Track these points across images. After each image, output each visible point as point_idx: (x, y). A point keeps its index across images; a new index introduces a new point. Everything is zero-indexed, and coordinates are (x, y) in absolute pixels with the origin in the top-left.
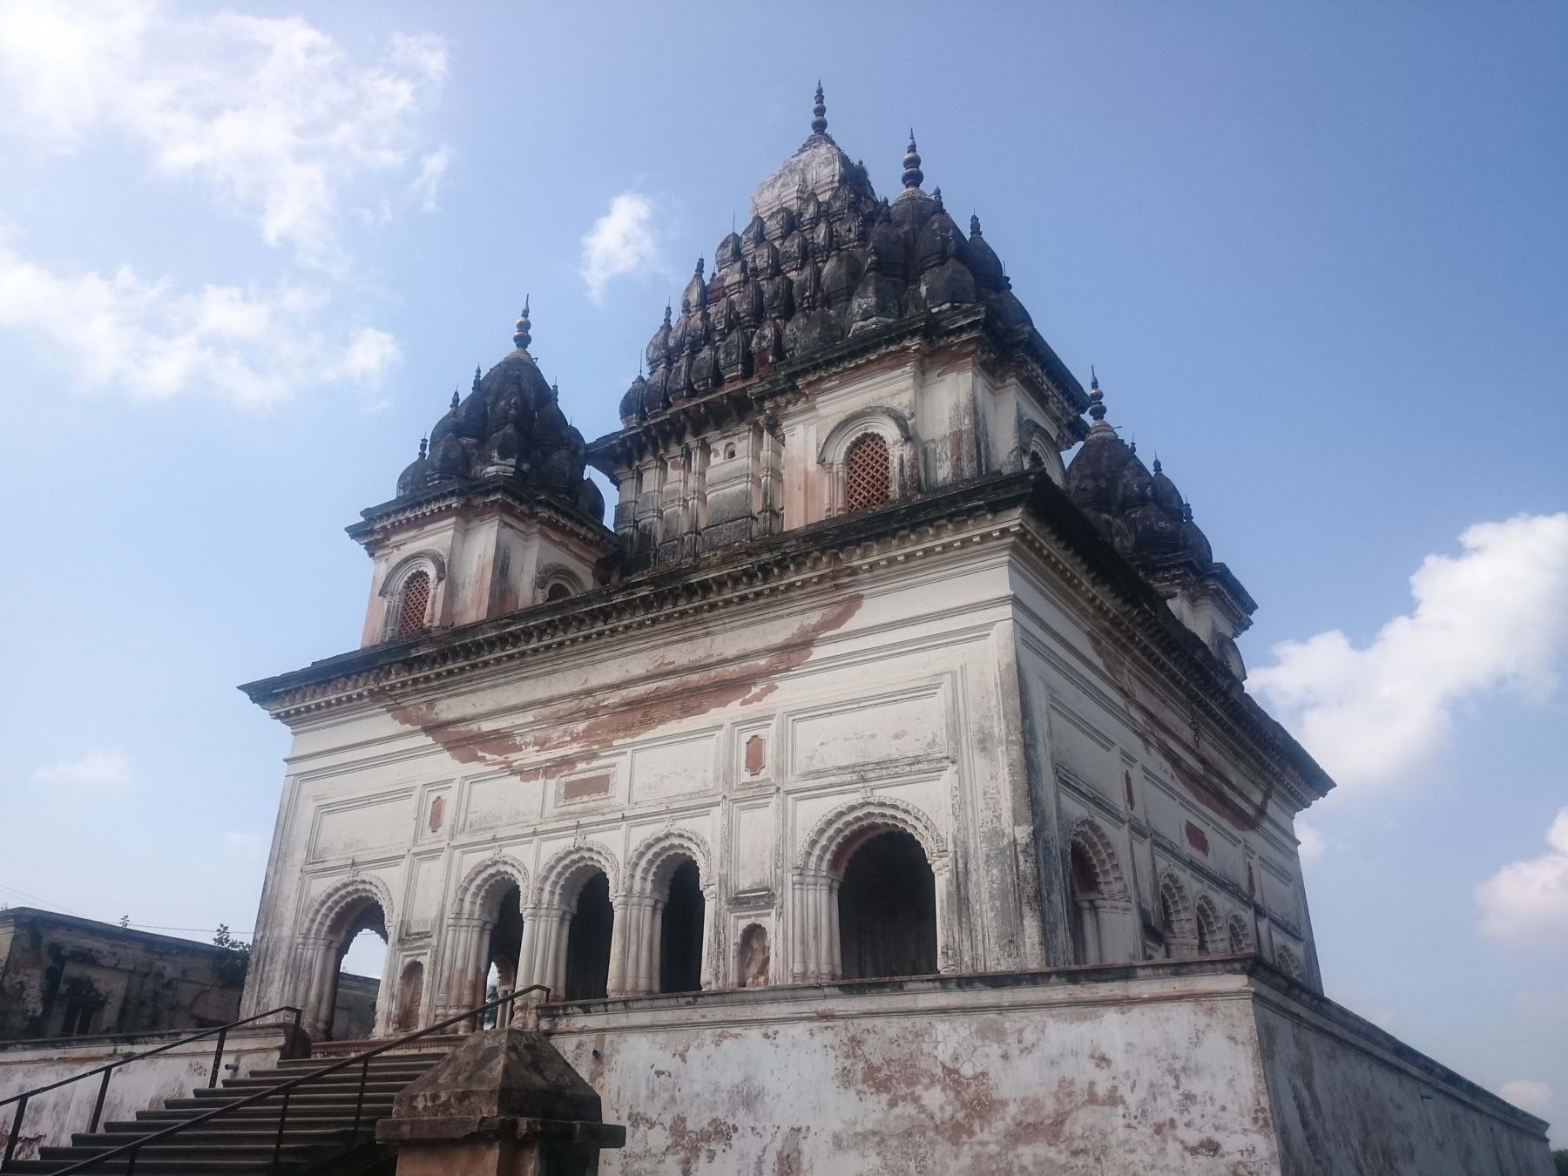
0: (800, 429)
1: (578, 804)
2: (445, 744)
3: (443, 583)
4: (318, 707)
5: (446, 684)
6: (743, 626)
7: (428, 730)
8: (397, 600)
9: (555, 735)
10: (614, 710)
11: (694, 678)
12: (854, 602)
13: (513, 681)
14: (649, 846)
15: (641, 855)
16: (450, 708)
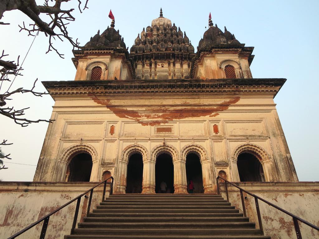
0: (209, 61)
1: (162, 134)
3: (106, 72)
4: (69, 93)
5: (116, 95)
6: (209, 98)
7: (108, 107)
8: (90, 72)
9: (152, 115)
10: (171, 112)
11: (196, 108)
12: (238, 99)
14: (187, 148)
15: (184, 150)
16: (114, 102)
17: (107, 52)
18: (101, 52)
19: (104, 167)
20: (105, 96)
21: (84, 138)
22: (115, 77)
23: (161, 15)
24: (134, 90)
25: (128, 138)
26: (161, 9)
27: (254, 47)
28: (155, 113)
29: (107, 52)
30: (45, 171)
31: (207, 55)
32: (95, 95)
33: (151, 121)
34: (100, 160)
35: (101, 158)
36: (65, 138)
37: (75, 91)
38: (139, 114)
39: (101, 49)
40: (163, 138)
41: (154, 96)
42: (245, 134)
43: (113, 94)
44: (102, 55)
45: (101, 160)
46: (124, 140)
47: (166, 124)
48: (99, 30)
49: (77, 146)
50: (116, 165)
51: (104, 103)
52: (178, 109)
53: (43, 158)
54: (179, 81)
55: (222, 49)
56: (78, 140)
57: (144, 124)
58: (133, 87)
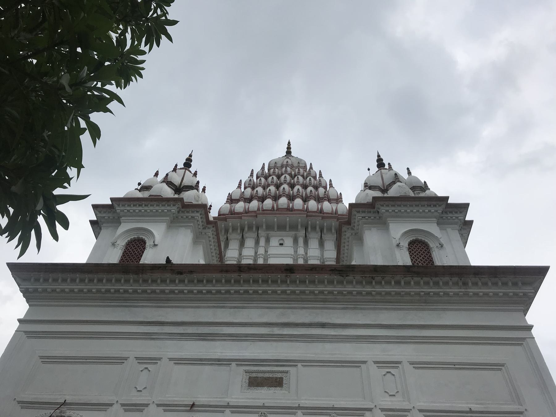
22: (168, 258)
23: (289, 152)
26: (289, 143)
27: (468, 205)
48: (158, 171)
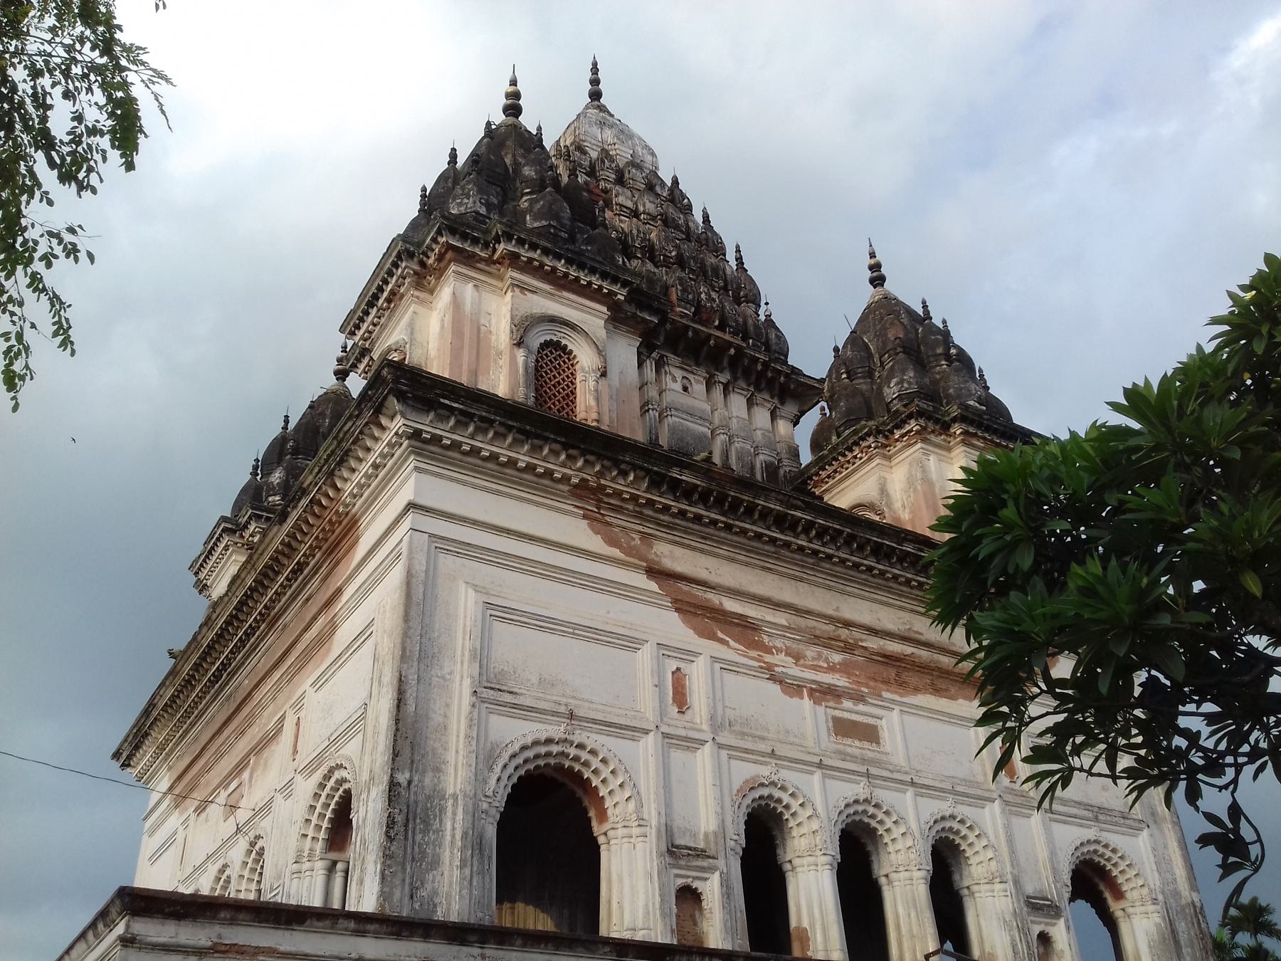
1: (854, 746)
2: (675, 601)
13: (754, 566)
17: (601, 287)
18: (577, 279)
19: (680, 868)
20: (640, 516)
21: (576, 706)
23: (596, 95)
24: (754, 528)
25: (748, 744)
26: (595, 65)
28: (819, 649)
29: (601, 287)
30: (423, 853)
31: (932, 437)
32: (600, 501)
33: (814, 682)
34: (659, 832)
35: (663, 821)
36: (494, 691)
37: (521, 457)
38: (766, 639)
39: (581, 266)
40: (863, 769)
41: (812, 569)
42: (1085, 800)
43: (670, 519)
44: (574, 292)
45: (663, 829)
46: (730, 747)
47: (861, 707)
49: (549, 741)
50: (721, 863)
51: (630, 547)
52: (891, 648)
53: (410, 782)
54: (911, 541)
55: (986, 435)
56: (555, 714)
57: (793, 688)
58: (756, 516)
